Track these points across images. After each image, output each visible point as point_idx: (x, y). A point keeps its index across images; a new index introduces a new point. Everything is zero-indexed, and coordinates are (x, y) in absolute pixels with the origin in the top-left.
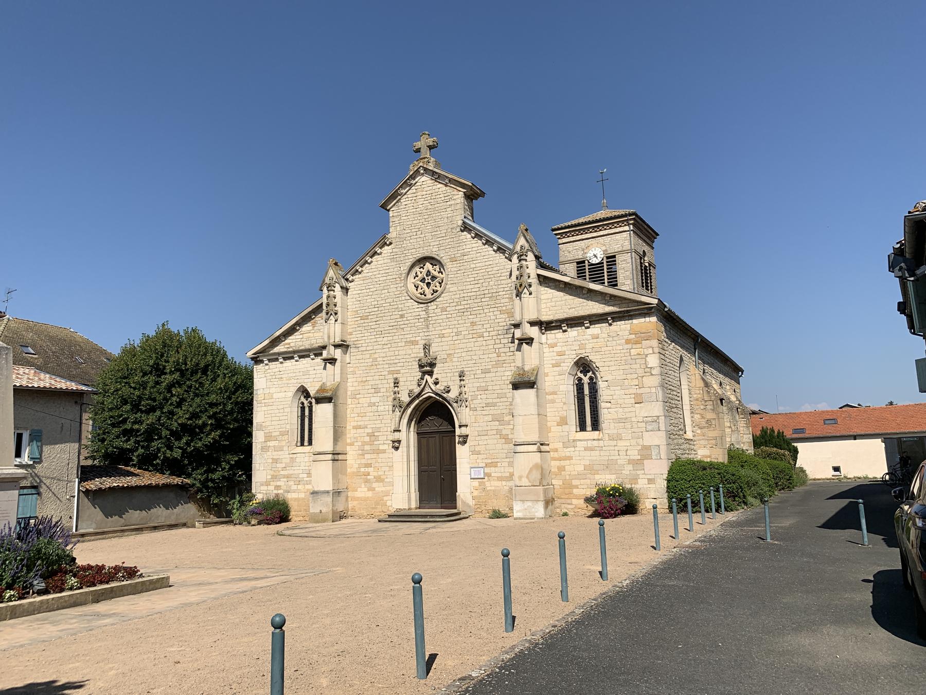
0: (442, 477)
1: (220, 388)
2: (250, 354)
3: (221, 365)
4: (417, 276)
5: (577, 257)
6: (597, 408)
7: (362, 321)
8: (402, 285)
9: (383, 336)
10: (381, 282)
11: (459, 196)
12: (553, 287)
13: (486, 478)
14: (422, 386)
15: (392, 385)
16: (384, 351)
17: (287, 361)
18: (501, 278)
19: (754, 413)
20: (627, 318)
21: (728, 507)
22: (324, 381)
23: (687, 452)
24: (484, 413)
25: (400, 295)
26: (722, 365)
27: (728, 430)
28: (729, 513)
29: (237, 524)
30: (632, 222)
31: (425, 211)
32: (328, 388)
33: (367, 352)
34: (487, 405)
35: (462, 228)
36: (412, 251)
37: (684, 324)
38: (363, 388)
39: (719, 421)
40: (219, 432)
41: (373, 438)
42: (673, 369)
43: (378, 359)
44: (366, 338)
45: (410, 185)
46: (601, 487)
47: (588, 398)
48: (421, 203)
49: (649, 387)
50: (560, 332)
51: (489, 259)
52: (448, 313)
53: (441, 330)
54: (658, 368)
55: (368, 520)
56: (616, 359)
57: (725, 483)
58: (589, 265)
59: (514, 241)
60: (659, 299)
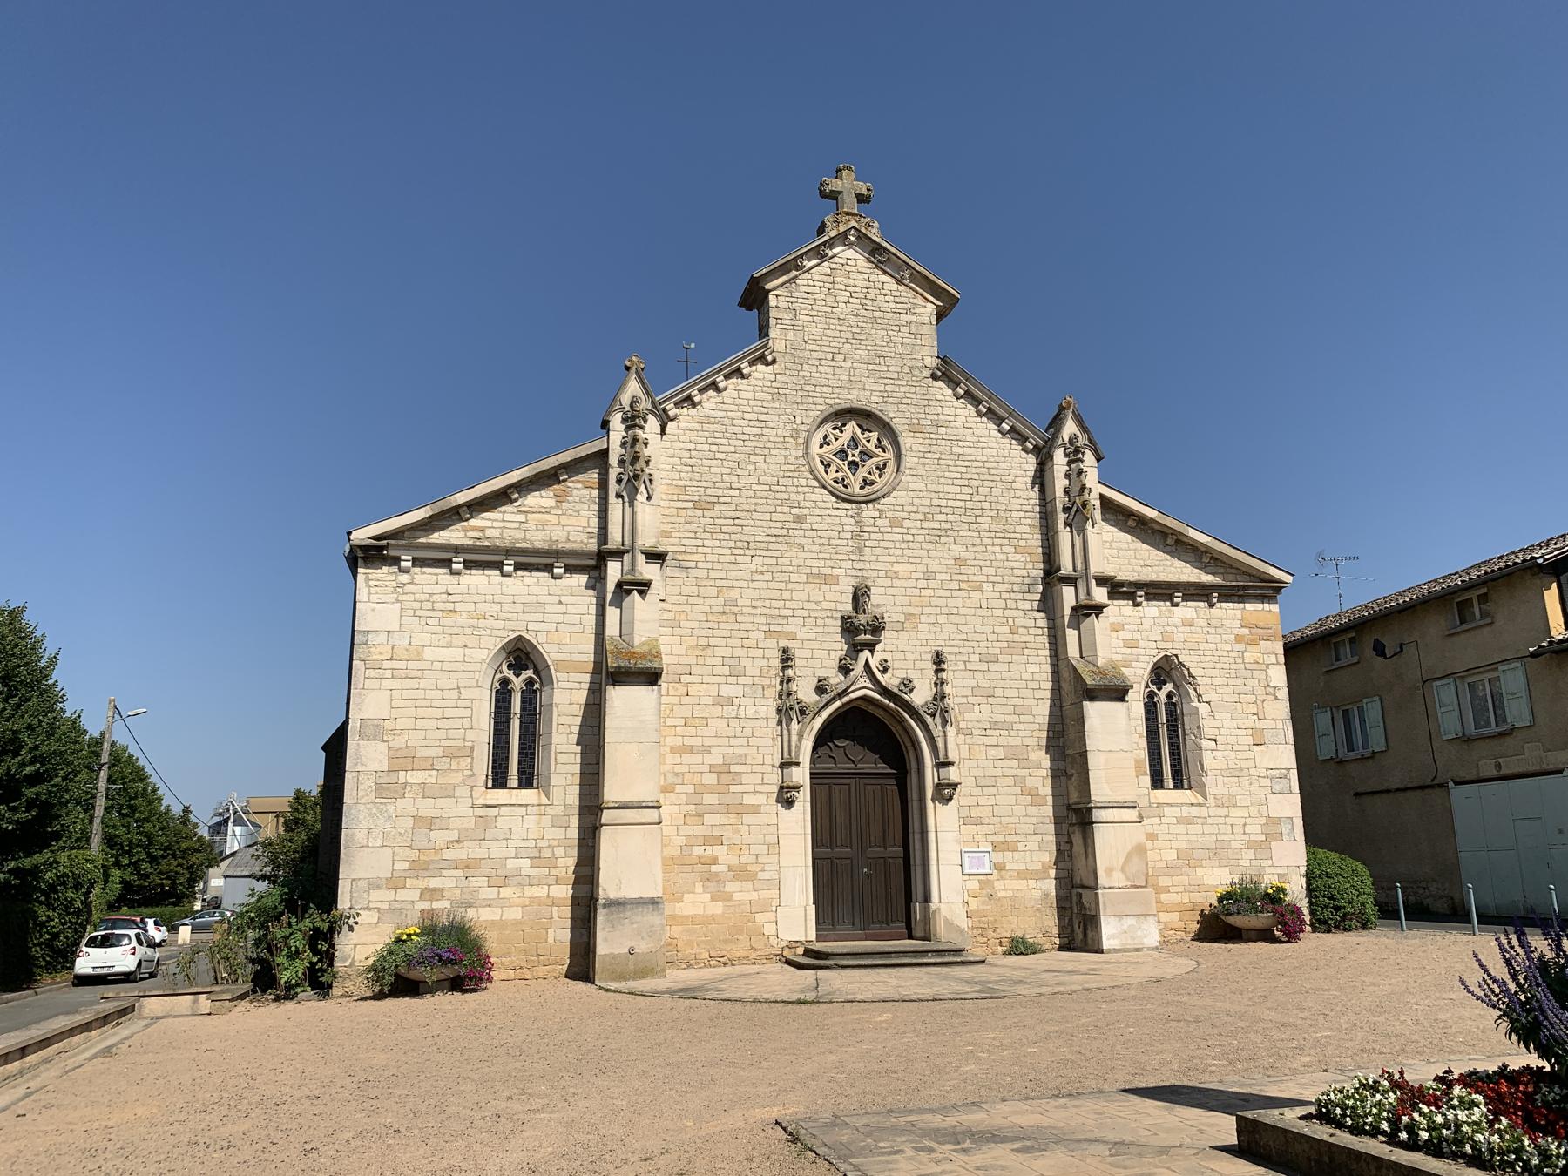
7: (699, 512)
10: (746, 437)
11: (927, 309)
16: (752, 585)
17: (473, 572)
24: (987, 741)
25: (796, 475)
31: (854, 318)
33: (712, 583)
34: (994, 726)
36: (825, 389)
38: (701, 661)
41: (725, 778)
43: (740, 602)
44: (709, 550)
49: (1273, 719)
52: (905, 531)
53: (892, 563)
56: (1222, 665)
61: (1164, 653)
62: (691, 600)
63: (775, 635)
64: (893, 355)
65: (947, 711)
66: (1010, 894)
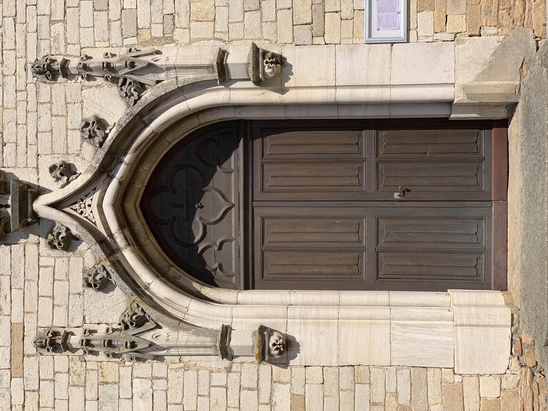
0: (396, 196)
63: (17, 359)
65: (132, 65)
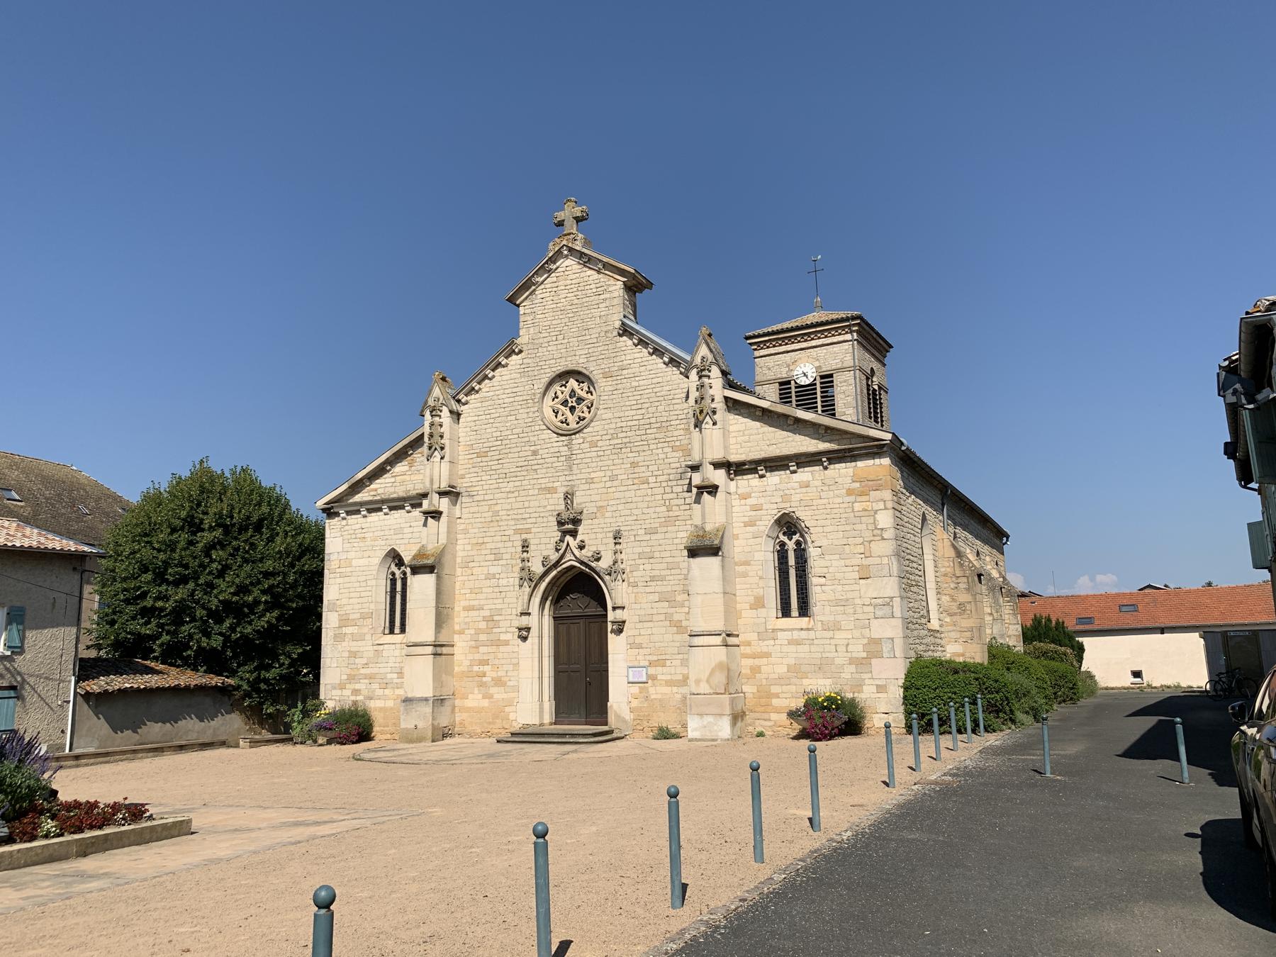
1: (280, 552)
2: (321, 503)
3: (281, 519)
4: (557, 398)
5: (779, 376)
6: (806, 585)
7: (479, 460)
8: (536, 409)
9: (508, 480)
11: (616, 287)
12: (746, 415)
13: (650, 681)
14: (561, 552)
15: (520, 549)
16: (509, 501)
17: (373, 514)
18: (674, 402)
19: (1023, 595)
20: (849, 459)
21: (989, 726)
22: (424, 542)
23: (932, 648)
24: (648, 590)
25: (533, 424)
26: (979, 527)
27: (988, 619)
28: (989, 734)
29: (297, 743)
30: (856, 328)
31: (570, 307)
32: (428, 552)
33: (486, 503)
34: (653, 579)
35: (621, 332)
37: (927, 470)
38: (479, 552)
39: (976, 605)
40: (276, 613)
42: (913, 532)
43: (501, 513)
44: (484, 483)
45: (549, 271)
46: (810, 696)
47: (794, 570)
48: (564, 296)
49: (879, 556)
50: (755, 478)
51: (658, 375)
52: (598, 449)
54: (892, 530)
55: (483, 740)
56: (833, 516)
57: (986, 692)
58: (796, 387)
59: (692, 350)
60: (893, 434)
61: (782, 512)
62: (475, 515)
64: (593, 326)
66: (659, 696)
